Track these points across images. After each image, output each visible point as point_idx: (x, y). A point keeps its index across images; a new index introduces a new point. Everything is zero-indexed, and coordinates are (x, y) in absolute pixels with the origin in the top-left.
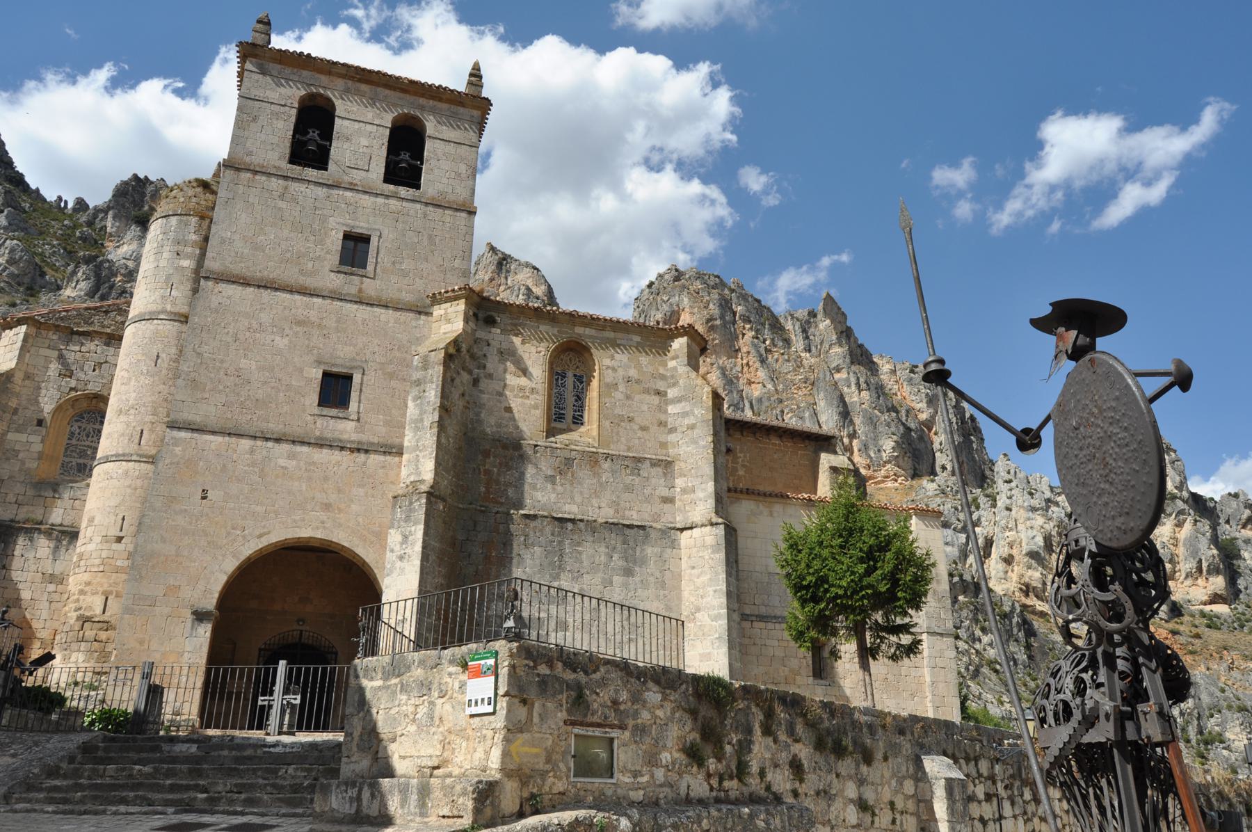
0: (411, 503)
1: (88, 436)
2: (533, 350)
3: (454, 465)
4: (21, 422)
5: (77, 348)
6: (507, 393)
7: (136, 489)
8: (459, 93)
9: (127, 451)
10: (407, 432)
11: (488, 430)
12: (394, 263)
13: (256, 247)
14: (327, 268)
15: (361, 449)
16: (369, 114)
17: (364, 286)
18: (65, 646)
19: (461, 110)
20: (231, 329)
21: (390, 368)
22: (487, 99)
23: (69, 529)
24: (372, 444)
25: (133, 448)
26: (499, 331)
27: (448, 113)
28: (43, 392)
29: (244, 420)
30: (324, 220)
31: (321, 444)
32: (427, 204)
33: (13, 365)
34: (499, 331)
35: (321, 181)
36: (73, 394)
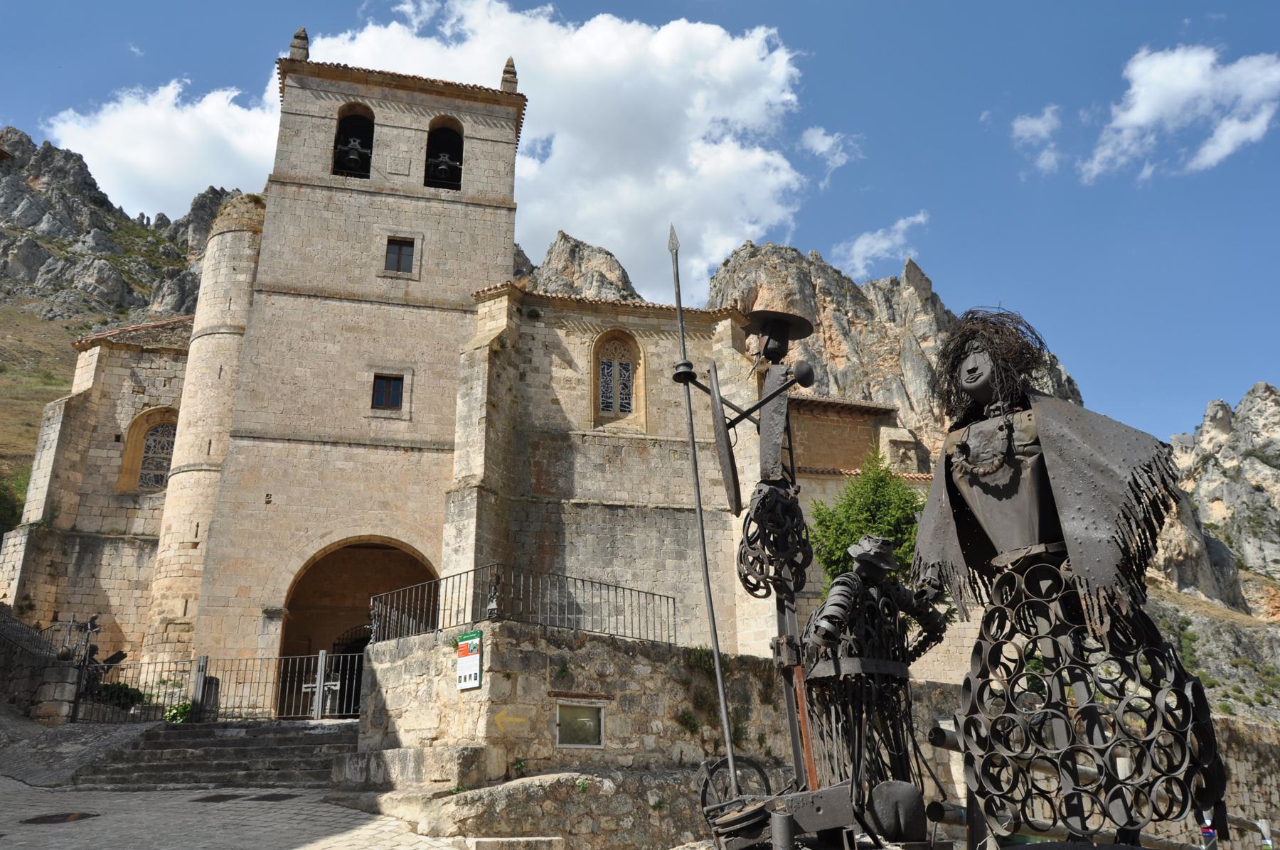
0: (463, 498)
1: (163, 449)
2: (578, 341)
3: (504, 459)
4: (100, 439)
5: (147, 365)
6: (554, 385)
7: (207, 497)
8: (494, 91)
9: (197, 462)
11: (537, 423)
12: (438, 264)
13: (306, 258)
14: (374, 274)
15: (415, 448)
16: (407, 119)
17: (410, 289)
18: (152, 647)
19: (497, 108)
21: (439, 368)
22: (522, 95)
23: (150, 538)
24: (425, 442)
25: (202, 458)
26: (543, 325)
27: (485, 112)
28: (119, 409)
29: (305, 426)
30: (368, 227)
31: (376, 445)
32: (467, 204)
33: (89, 385)
34: (543, 325)
35: (363, 189)
36: (147, 409)
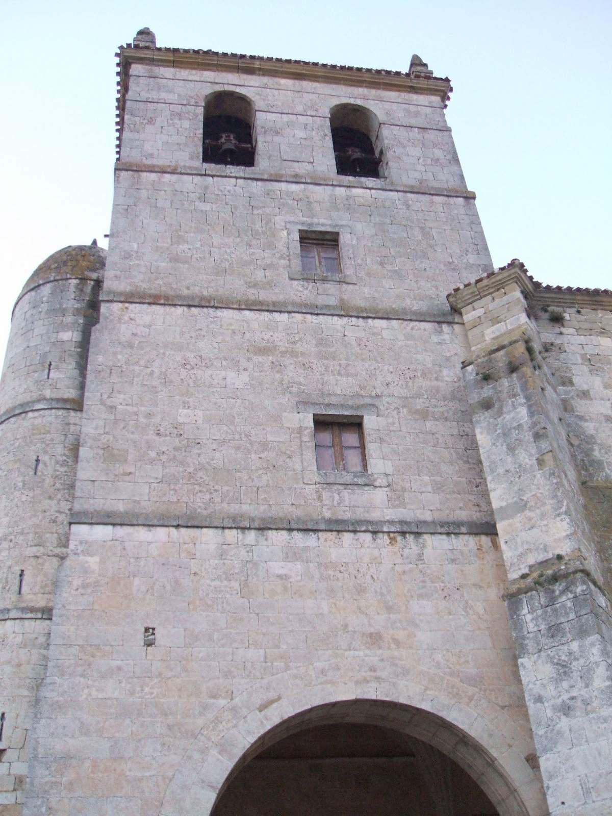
0: (552, 600)
7: (19, 665)
10: (491, 486)
13: (175, 259)
19: (414, 97)
20: (156, 368)
21: (420, 404)
30: (267, 221)
31: (337, 526)
34: (571, 331)
